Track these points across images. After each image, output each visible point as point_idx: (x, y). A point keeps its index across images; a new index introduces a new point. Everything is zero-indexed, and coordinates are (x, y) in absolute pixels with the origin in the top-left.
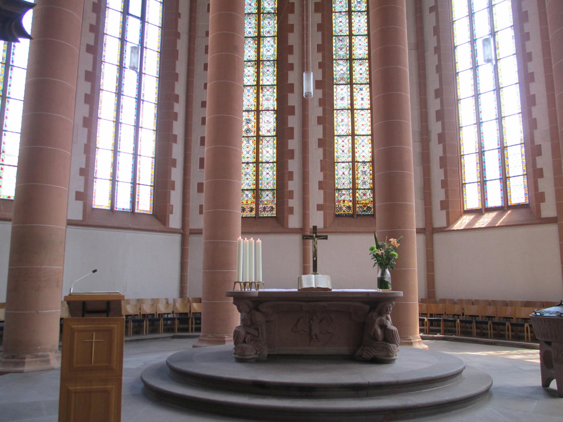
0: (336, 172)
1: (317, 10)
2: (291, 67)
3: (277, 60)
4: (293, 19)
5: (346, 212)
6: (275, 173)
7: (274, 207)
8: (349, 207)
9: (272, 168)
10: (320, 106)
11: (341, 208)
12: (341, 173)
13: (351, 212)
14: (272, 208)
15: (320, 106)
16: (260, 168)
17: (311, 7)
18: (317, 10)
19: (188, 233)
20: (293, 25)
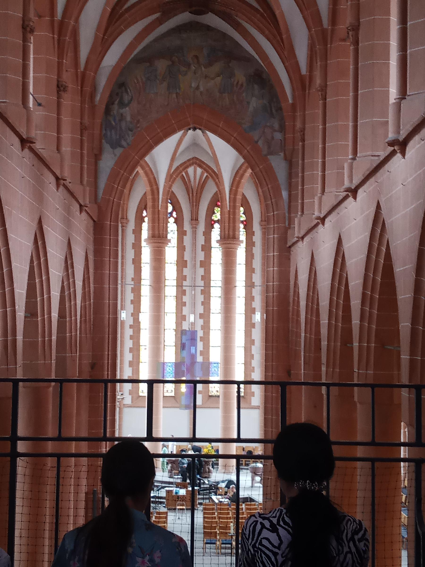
0: (210, 369)
1: (201, 266)
2: (184, 304)
3: (176, 296)
4: (186, 271)
5: (216, 394)
6: (174, 369)
7: (173, 390)
8: (217, 391)
9: (172, 366)
10: (202, 329)
11: (212, 392)
12: (213, 370)
13: (218, 394)
14: (172, 391)
15: (202, 329)
16: (165, 366)
17: (198, 264)
18: (201, 266)
19: (122, 406)
20: (186, 276)
